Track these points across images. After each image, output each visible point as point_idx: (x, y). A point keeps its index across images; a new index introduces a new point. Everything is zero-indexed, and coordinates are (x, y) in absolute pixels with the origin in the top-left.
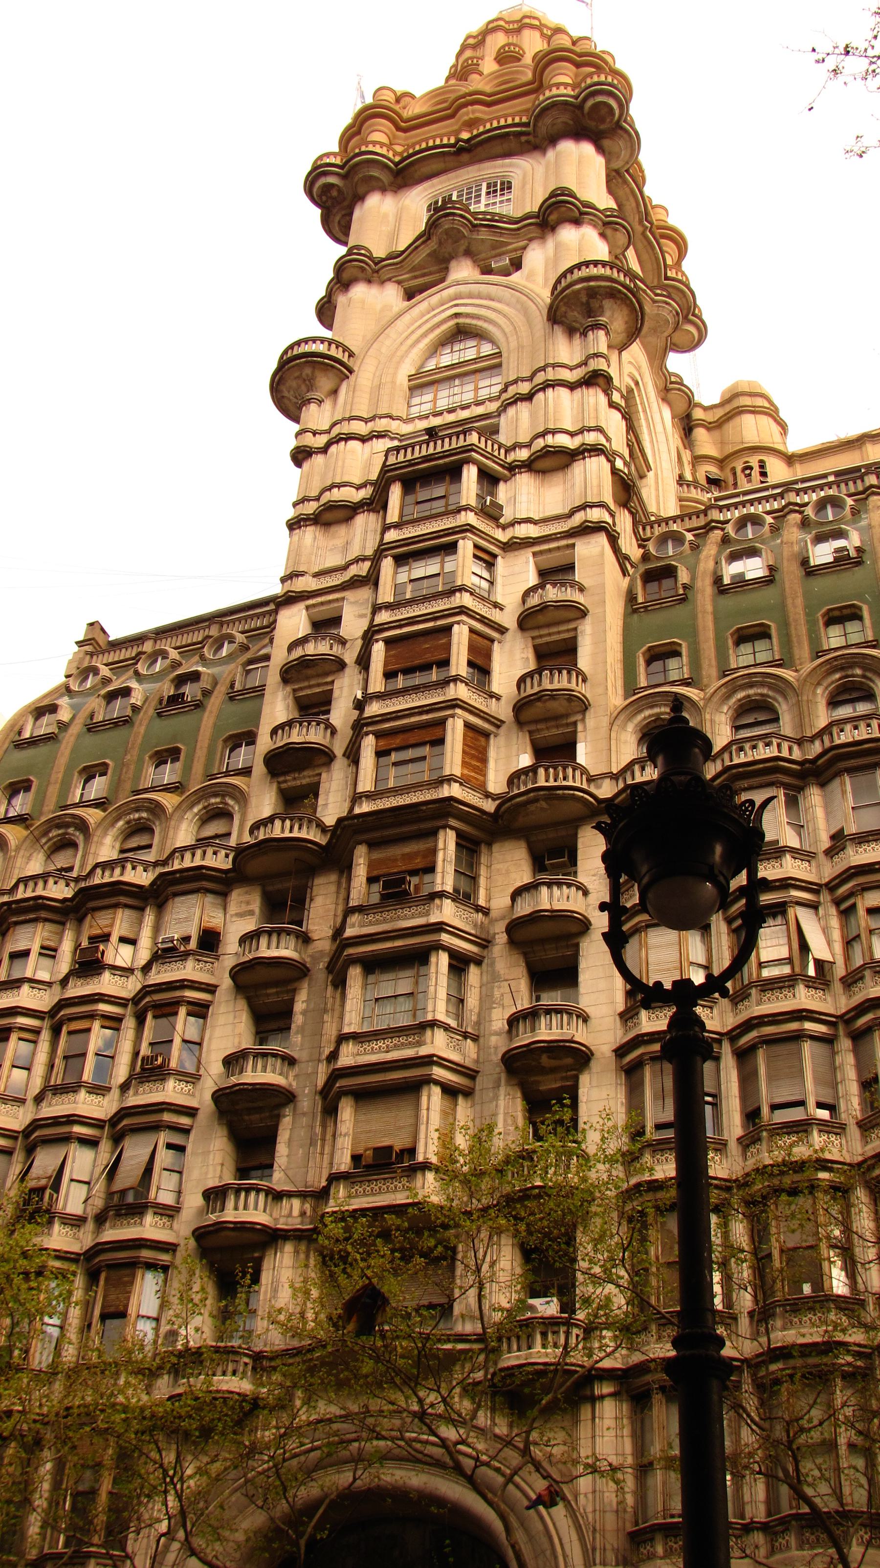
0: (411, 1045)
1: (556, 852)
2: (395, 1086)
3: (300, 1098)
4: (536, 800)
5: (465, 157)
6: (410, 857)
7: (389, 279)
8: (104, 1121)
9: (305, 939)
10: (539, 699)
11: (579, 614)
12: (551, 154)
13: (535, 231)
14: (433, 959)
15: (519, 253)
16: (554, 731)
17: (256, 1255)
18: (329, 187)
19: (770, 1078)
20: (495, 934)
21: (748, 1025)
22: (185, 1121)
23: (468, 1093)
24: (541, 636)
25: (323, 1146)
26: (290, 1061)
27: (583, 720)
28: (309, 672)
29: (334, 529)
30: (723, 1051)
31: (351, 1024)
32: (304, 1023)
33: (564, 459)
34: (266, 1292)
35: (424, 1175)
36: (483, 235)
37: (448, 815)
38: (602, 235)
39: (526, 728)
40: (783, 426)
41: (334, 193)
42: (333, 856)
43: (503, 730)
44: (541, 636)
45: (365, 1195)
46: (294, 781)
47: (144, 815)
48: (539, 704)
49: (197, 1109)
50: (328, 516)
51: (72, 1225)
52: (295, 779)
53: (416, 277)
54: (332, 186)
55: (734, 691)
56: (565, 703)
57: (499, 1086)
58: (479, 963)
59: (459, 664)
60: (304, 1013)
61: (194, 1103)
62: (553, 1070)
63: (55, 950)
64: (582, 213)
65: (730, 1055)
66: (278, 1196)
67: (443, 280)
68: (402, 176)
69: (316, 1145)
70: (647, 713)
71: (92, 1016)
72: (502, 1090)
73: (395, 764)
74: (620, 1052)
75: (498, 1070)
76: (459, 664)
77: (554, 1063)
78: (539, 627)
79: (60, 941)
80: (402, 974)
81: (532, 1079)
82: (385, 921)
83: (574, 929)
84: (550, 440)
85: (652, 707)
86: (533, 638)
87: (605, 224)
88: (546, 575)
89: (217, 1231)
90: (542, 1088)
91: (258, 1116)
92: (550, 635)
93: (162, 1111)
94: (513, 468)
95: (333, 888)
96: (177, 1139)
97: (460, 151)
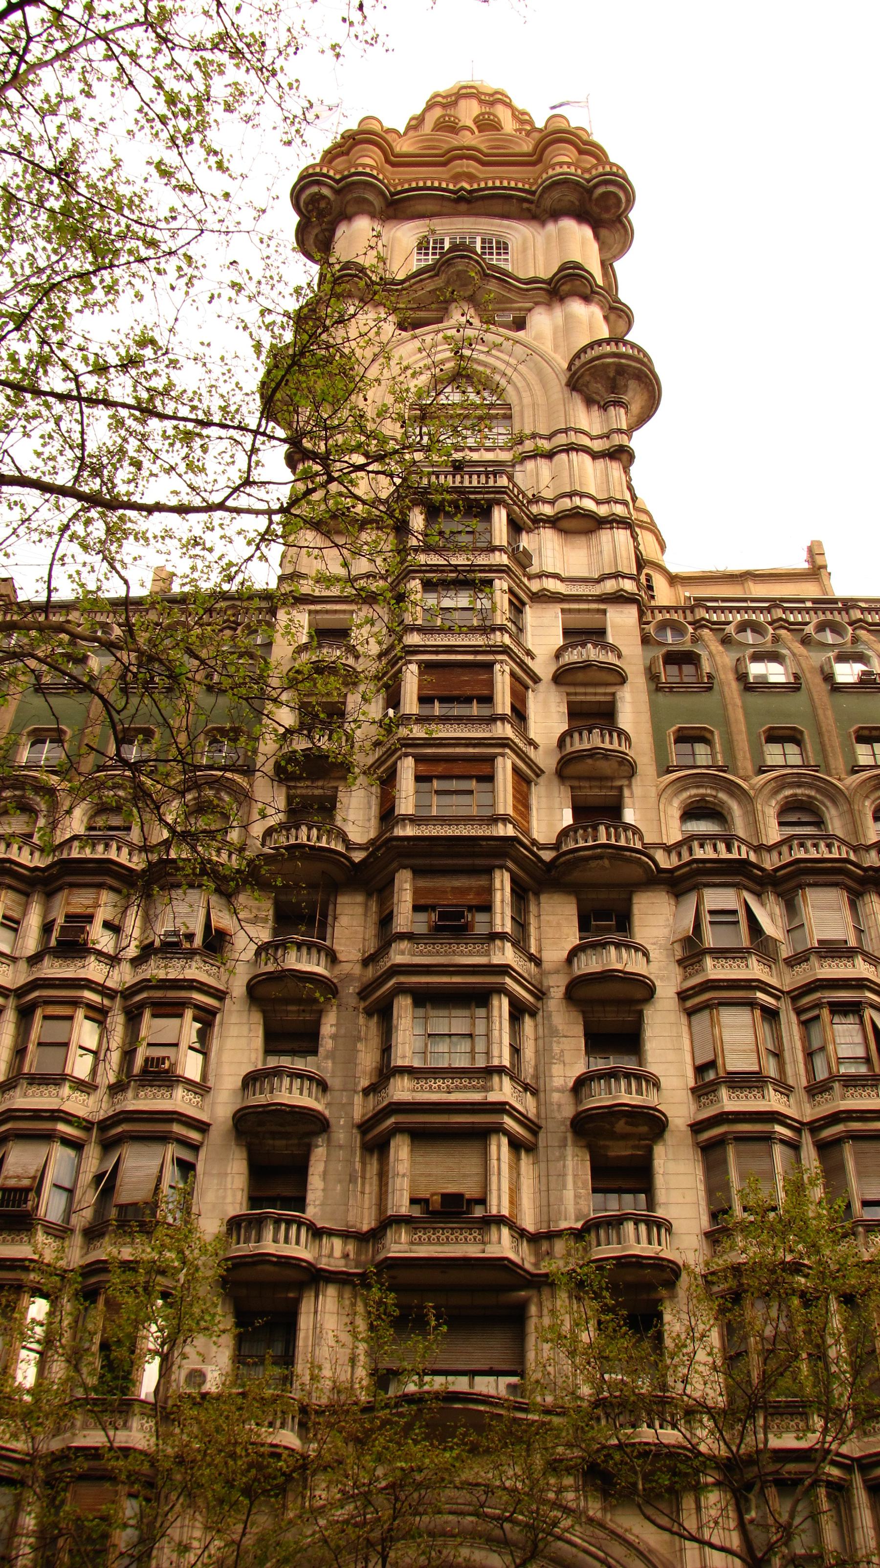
0: (475, 1089)
1: (603, 914)
2: (462, 1130)
3: (334, 1128)
4: (600, 857)
5: (463, 207)
6: (461, 891)
8: (92, 1123)
9: (333, 958)
10: (591, 756)
11: (619, 679)
12: (551, 227)
13: (542, 296)
14: (495, 1002)
15: (522, 314)
16: (596, 792)
17: (291, 1295)
18: (316, 199)
19: (860, 1174)
20: (549, 987)
21: (835, 1118)
22: (194, 1135)
23: (531, 1149)
24: (576, 694)
25: (363, 1184)
26: (323, 1086)
27: (630, 786)
30: (804, 1140)
31: (404, 1057)
32: (335, 1049)
33: (590, 524)
34: (306, 1338)
35: (499, 1230)
36: (493, 286)
37: (505, 855)
38: (606, 318)
39: (568, 783)
40: (662, 547)
41: (323, 205)
42: (369, 875)
43: (542, 780)
44: (576, 694)
45: (430, 1243)
46: (304, 788)
48: (589, 761)
49: (209, 1125)
51: (56, 1236)
54: (324, 197)
55: (782, 787)
56: (615, 765)
57: (565, 1146)
58: (533, 1014)
59: (503, 703)
60: (334, 1037)
61: (204, 1117)
62: (625, 1137)
63: (18, 922)
64: (593, 292)
65: (811, 1147)
66: (317, 1233)
67: (440, 321)
68: (395, 208)
69: (356, 1183)
70: (693, 792)
71: (75, 1003)
72: (569, 1151)
73: (437, 792)
74: (697, 1128)
75: (563, 1128)
76: (503, 703)
77: (629, 1129)
78: (574, 684)
79: (25, 914)
80: (454, 1013)
81: (602, 1143)
82: (438, 953)
83: (639, 994)
84: (577, 501)
85: (698, 787)
86: (568, 694)
87: (612, 308)
88: (574, 635)
89: (254, 1264)
90: (611, 1154)
91: (284, 1142)
92: (585, 694)
93: (171, 1121)
94: (538, 521)
95: (360, 910)
96: (186, 1155)
97: (461, 199)
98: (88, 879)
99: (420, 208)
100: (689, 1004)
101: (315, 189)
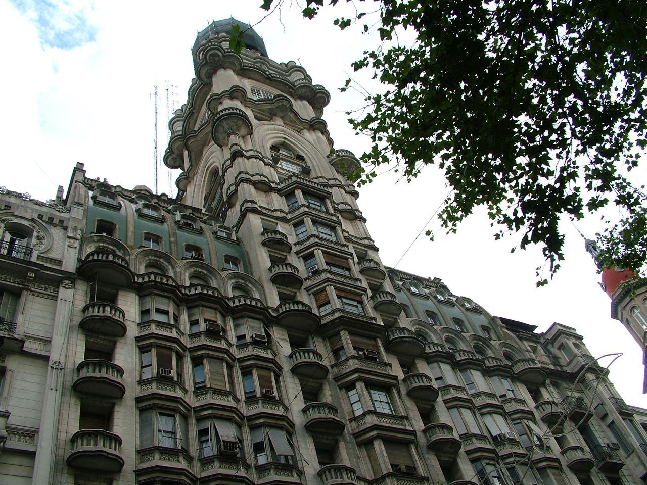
5: (268, 81)
7: (249, 107)
13: (308, 127)
28: (277, 246)
29: (259, 192)
36: (292, 115)
47: (205, 272)
50: (260, 186)
52: (284, 289)
53: (259, 113)
54: (219, 55)
97: (269, 78)
98: (213, 305)
99: (252, 76)
100: (448, 405)
101: (216, 51)
